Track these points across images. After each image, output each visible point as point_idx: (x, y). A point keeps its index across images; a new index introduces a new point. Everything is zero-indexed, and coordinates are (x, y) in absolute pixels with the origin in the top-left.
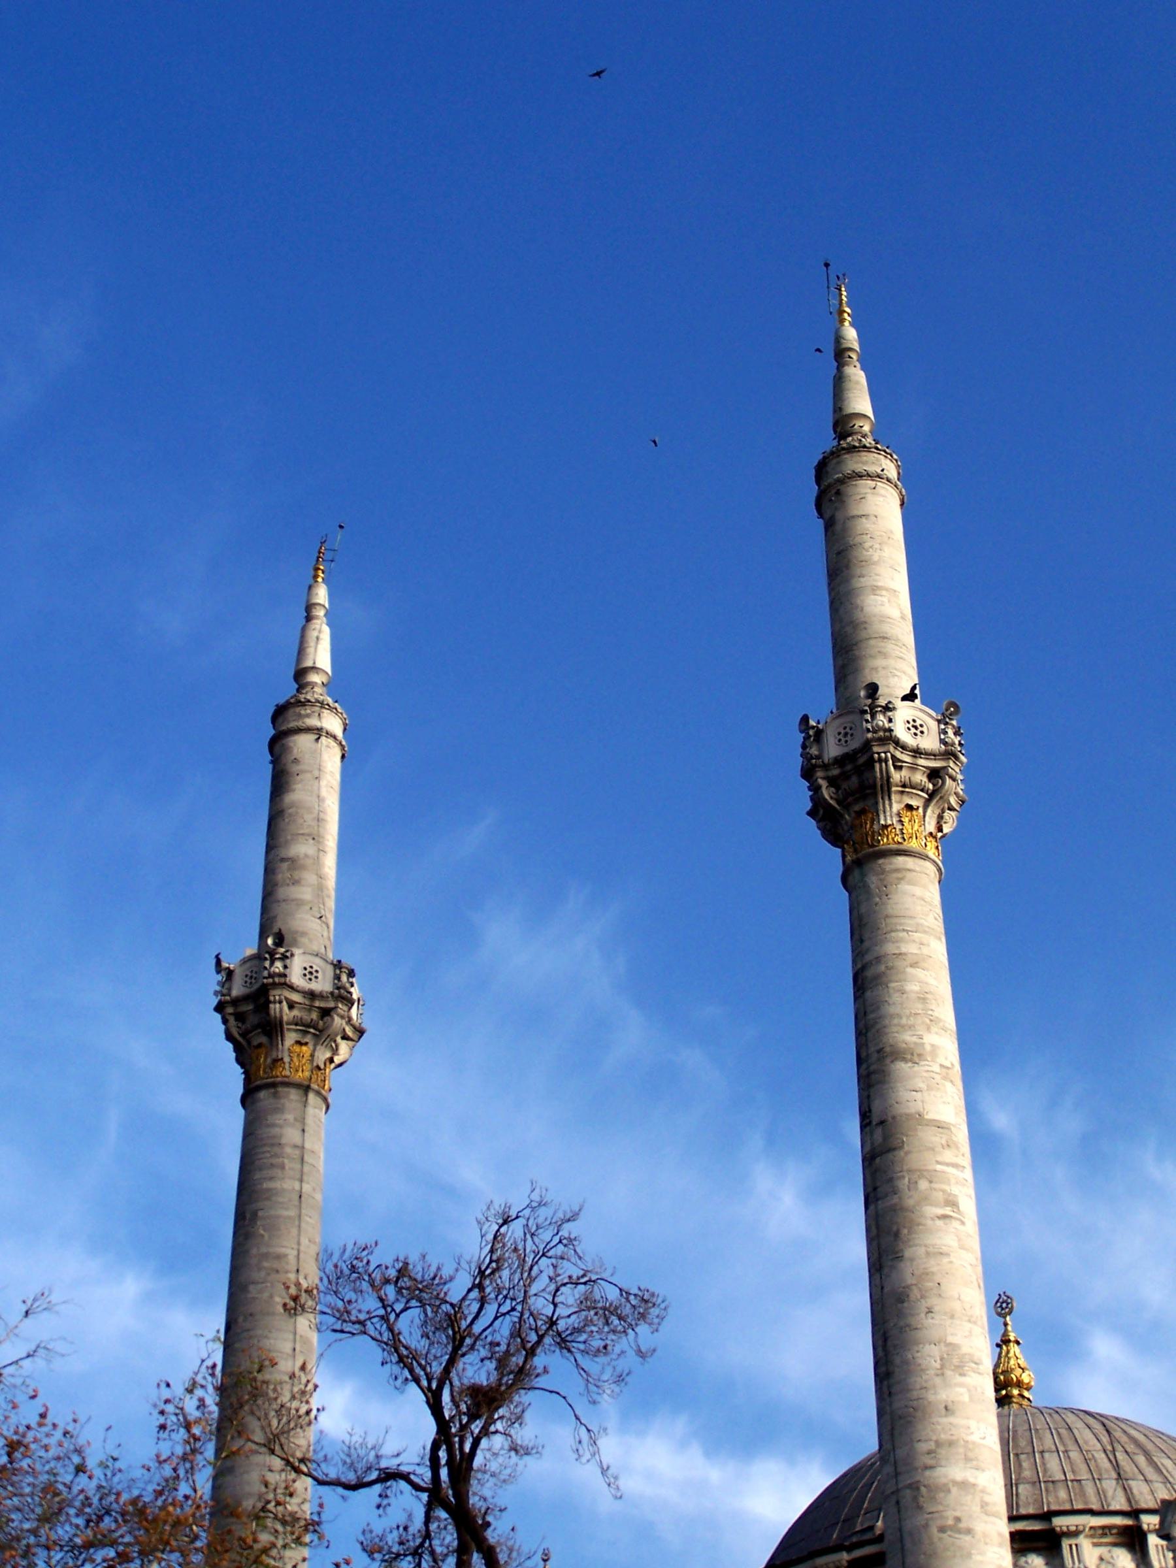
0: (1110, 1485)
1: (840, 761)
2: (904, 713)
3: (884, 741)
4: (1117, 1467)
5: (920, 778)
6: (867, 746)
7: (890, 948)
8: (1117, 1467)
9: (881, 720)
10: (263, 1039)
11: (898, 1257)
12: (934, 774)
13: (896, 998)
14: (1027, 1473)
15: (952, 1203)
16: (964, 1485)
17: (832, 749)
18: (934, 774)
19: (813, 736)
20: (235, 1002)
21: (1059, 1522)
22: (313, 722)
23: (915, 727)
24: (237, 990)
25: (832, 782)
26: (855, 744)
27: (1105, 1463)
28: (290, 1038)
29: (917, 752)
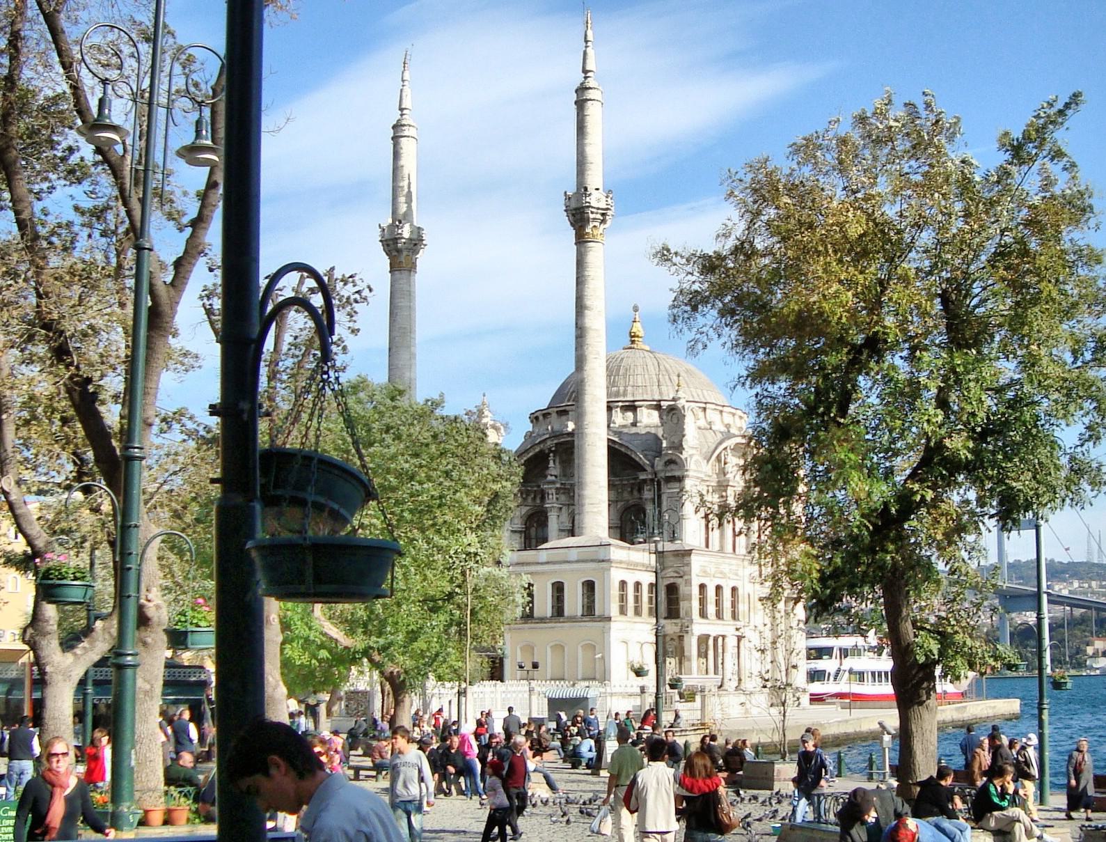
0: (655, 388)
2: (595, 194)
3: (588, 207)
5: (599, 216)
6: (583, 207)
7: (586, 273)
9: (588, 199)
12: (603, 214)
14: (631, 383)
15: (598, 354)
17: (573, 205)
18: (603, 214)
21: (637, 403)
22: (406, 133)
23: (599, 200)
24: (387, 237)
25: (573, 215)
26: (579, 205)
27: (655, 380)
28: (405, 253)
29: (598, 209)
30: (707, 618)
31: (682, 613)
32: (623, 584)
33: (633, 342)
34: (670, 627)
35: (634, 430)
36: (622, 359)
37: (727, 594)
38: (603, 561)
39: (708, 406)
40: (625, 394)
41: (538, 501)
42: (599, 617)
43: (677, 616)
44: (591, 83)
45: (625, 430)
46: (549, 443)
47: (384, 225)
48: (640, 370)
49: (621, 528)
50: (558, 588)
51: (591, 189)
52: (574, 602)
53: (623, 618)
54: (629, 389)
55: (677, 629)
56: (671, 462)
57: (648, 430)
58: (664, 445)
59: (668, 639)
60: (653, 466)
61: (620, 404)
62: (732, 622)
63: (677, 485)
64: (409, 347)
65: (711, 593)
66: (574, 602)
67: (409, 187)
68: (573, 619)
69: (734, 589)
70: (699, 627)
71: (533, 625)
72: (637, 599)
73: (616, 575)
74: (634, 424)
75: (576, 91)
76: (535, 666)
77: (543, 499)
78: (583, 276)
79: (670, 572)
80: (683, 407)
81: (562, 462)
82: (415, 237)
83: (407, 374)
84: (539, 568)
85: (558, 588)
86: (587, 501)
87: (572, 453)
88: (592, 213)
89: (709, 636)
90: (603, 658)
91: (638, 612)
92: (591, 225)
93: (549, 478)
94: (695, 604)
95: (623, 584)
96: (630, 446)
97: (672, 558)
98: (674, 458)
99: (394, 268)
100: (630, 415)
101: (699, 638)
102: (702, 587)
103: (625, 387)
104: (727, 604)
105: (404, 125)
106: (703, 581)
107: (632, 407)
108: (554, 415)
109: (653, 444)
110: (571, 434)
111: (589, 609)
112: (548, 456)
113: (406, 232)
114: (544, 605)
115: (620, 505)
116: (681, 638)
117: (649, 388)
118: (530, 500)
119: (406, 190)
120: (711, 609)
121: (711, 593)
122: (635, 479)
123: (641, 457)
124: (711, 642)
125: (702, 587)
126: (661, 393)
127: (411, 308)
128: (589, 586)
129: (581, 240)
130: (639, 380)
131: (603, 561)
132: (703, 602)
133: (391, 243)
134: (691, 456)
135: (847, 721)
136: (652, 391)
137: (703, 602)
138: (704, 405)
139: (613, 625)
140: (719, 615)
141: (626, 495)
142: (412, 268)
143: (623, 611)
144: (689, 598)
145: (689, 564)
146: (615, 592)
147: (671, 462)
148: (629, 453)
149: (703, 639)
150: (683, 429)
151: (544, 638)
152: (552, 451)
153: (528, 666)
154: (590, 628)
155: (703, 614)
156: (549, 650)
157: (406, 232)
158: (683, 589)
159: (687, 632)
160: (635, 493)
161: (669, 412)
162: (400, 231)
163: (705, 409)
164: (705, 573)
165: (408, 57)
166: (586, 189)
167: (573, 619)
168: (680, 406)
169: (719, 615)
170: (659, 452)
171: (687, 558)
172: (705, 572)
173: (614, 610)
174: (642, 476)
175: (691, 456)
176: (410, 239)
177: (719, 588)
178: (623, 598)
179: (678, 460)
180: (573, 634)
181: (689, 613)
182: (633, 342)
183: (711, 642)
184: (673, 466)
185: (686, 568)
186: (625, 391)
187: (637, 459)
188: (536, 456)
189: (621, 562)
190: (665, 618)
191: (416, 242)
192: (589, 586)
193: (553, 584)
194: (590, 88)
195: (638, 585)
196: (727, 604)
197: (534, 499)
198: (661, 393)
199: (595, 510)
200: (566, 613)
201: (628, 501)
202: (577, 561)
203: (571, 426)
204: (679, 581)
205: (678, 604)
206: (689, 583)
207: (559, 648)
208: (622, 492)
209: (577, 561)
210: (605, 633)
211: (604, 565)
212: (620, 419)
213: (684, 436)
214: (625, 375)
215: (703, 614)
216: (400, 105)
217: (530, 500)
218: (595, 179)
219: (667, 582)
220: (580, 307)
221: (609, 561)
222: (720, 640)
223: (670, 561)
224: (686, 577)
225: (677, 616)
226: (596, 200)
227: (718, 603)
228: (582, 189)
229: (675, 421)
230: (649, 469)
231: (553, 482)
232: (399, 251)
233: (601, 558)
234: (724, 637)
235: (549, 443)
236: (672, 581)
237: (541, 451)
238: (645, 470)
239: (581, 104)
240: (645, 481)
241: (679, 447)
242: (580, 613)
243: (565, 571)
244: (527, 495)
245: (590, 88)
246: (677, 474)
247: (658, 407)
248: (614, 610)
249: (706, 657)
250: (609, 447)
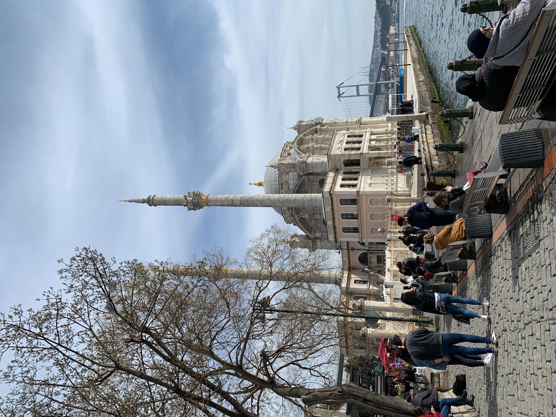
16: (283, 199)
19: (190, 209)
37: (351, 139)
52: (351, 209)
65: (349, 146)
66: (351, 209)
69: (349, 136)
70: (365, 149)
73: (338, 188)
91: (356, 179)
94: (353, 152)
100: (284, 186)
102: (346, 149)
104: (355, 139)
106: (343, 149)
111: (354, 202)
114: (352, 223)
120: (357, 145)
121: (349, 146)
137: (353, 149)
141: (315, 187)
143: (354, 186)
149: (371, 148)
154: (364, 202)
160: (314, 183)
172: (339, 149)
173: (354, 190)
177: (347, 143)
178: (349, 186)
180: (365, 208)
195: (343, 179)
196: (355, 139)
206: (343, 155)
215: (358, 149)
227: (354, 142)
234: (371, 140)
236: (342, 164)
237: (299, 220)
242: (356, 206)
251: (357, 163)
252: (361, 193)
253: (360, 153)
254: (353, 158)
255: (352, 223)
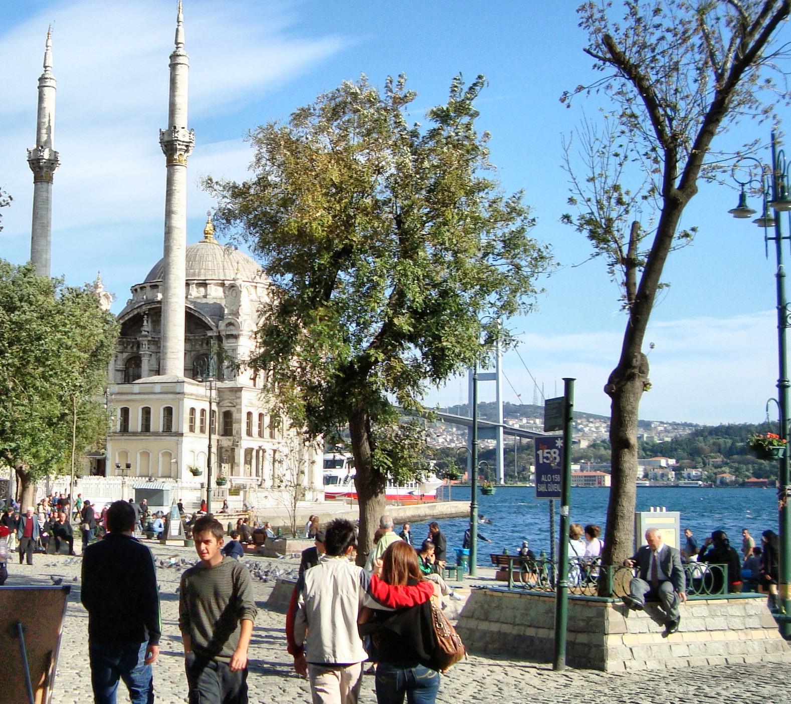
0: (221, 271)
1: (168, 142)
2: (181, 131)
4: (223, 266)
7: (174, 188)
8: (223, 266)
9: (176, 135)
10: (38, 170)
11: (169, 256)
12: (187, 146)
13: (173, 199)
17: (166, 138)
19: (163, 134)
20: (32, 160)
21: (207, 282)
24: (33, 157)
25: (165, 146)
28: (45, 170)
29: (183, 142)
30: (252, 436)
31: (234, 432)
32: (193, 410)
33: (206, 237)
34: (226, 442)
35: (204, 301)
36: (198, 250)
38: (179, 393)
39: (258, 285)
40: (199, 275)
41: (135, 349)
42: (175, 433)
43: (231, 434)
44: (181, 51)
45: (199, 301)
46: (144, 308)
47: (31, 149)
48: (210, 258)
49: (193, 370)
50: (147, 412)
51: (178, 128)
52: (157, 422)
53: (192, 434)
54: (202, 271)
55: (230, 443)
56: (230, 324)
57: (215, 301)
58: (226, 312)
59: (223, 450)
60: (217, 327)
61: (196, 282)
62: (270, 440)
63: (234, 340)
64: (46, 237)
66: (157, 422)
67: (49, 123)
68: (156, 434)
70: (246, 442)
71: (127, 437)
72: (202, 421)
73: (188, 404)
74: (205, 297)
75: (170, 57)
76: (128, 466)
77: (138, 347)
78: (171, 189)
79: (226, 403)
80: (240, 285)
81: (153, 322)
82: (52, 158)
83: (44, 256)
84: (133, 397)
85: (147, 412)
86: (169, 350)
87: (160, 316)
88: (179, 145)
89: (253, 449)
90: (177, 462)
91: (202, 430)
92: (178, 153)
93: (144, 333)
95: (193, 410)
96: (202, 312)
97: (228, 393)
98: (233, 321)
99: (38, 179)
100: (202, 289)
101: (246, 450)
102: (249, 414)
103: (200, 269)
105: (47, 78)
107: (204, 284)
108: (148, 288)
109: (218, 312)
110: (159, 302)
112: (143, 317)
113: (46, 155)
115: (193, 353)
116: (233, 450)
117: (216, 271)
118: (129, 347)
119: (47, 124)
120: (255, 430)
122: (204, 335)
123: (209, 321)
124: (254, 453)
125: (249, 414)
126: (225, 275)
127: (48, 210)
128: (169, 411)
129: (171, 164)
130: (210, 265)
131: (179, 393)
132: (249, 424)
133: (35, 162)
134: (245, 320)
135: (348, 513)
136: (219, 273)
137: (249, 424)
138: (255, 284)
139: (184, 439)
140: (261, 435)
141: (197, 347)
142: (50, 180)
143: (192, 429)
144: (239, 422)
145: (240, 398)
146: (186, 415)
147: (230, 324)
148: (201, 317)
149: (249, 452)
150: (240, 301)
151: (135, 447)
152: (145, 314)
153: (123, 466)
154: (169, 440)
155: (249, 433)
156: (138, 455)
157: (46, 155)
158: (235, 415)
159: (237, 446)
160: (204, 345)
161: (230, 289)
162: (42, 154)
163: (256, 287)
164: (252, 405)
165: (51, 30)
166: (175, 128)
167: (156, 434)
168: (238, 285)
169: (261, 435)
170: (221, 316)
171: (238, 393)
172: (251, 403)
173: (185, 428)
174: (210, 334)
175: (245, 320)
176: (49, 160)
178: (192, 420)
179: (236, 323)
180: (157, 445)
181: (239, 433)
182: (206, 237)
183: (254, 453)
184: (231, 327)
185: (238, 401)
186: (199, 272)
187: (206, 321)
188: (134, 317)
189: (191, 395)
190: (222, 435)
191: (53, 163)
192: (169, 411)
193: (143, 409)
194: (180, 55)
197: (132, 348)
198: (225, 275)
199: (175, 357)
200: (152, 429)
201: (199, 351)
202: (161, 393)
203: (160, 297)
204: (233, 409)
205: (232, 426)
206: (240, 411)
207: (146, 454)
208: (195, 345)
209: (161, 393)
210: (178, 444)
211: (178, 396)
212: (195, 292)
213: (240, 306)
214: (199, 261)
215: (249, 433)
216: (45, 64)
217: (129, 347)
218: (182, 120)
219: (224, 410)
220: (169, 213)
221: (183, 393)
222: (261, 452)
223: (227, 394)
224: (238, 407)
225: (231, 434)
226: (182, 135)
228: (173, 128)
229: (234, 295)
230: (215, 329)
231: (146, 336)
232: (41, 168)
233: (178, 391)
235: (144, 308)
236: (228, 409)
237: (138, 314)
238: (212, 329)
239: (173, 66)
240: (211, 337)
241: (236, 314)
242: (161, 430)
243: (151, 400)
244: (128, 345)
245: (180, 55)
246: (234, 333)
247: (223, 285)
248: (185, 428)
249: (251, 465)
250: (186, 313)
251: (227, 430)
252: (180, 438)
253: (242, 435)
254: (235, 426)
255: (135, 422)
